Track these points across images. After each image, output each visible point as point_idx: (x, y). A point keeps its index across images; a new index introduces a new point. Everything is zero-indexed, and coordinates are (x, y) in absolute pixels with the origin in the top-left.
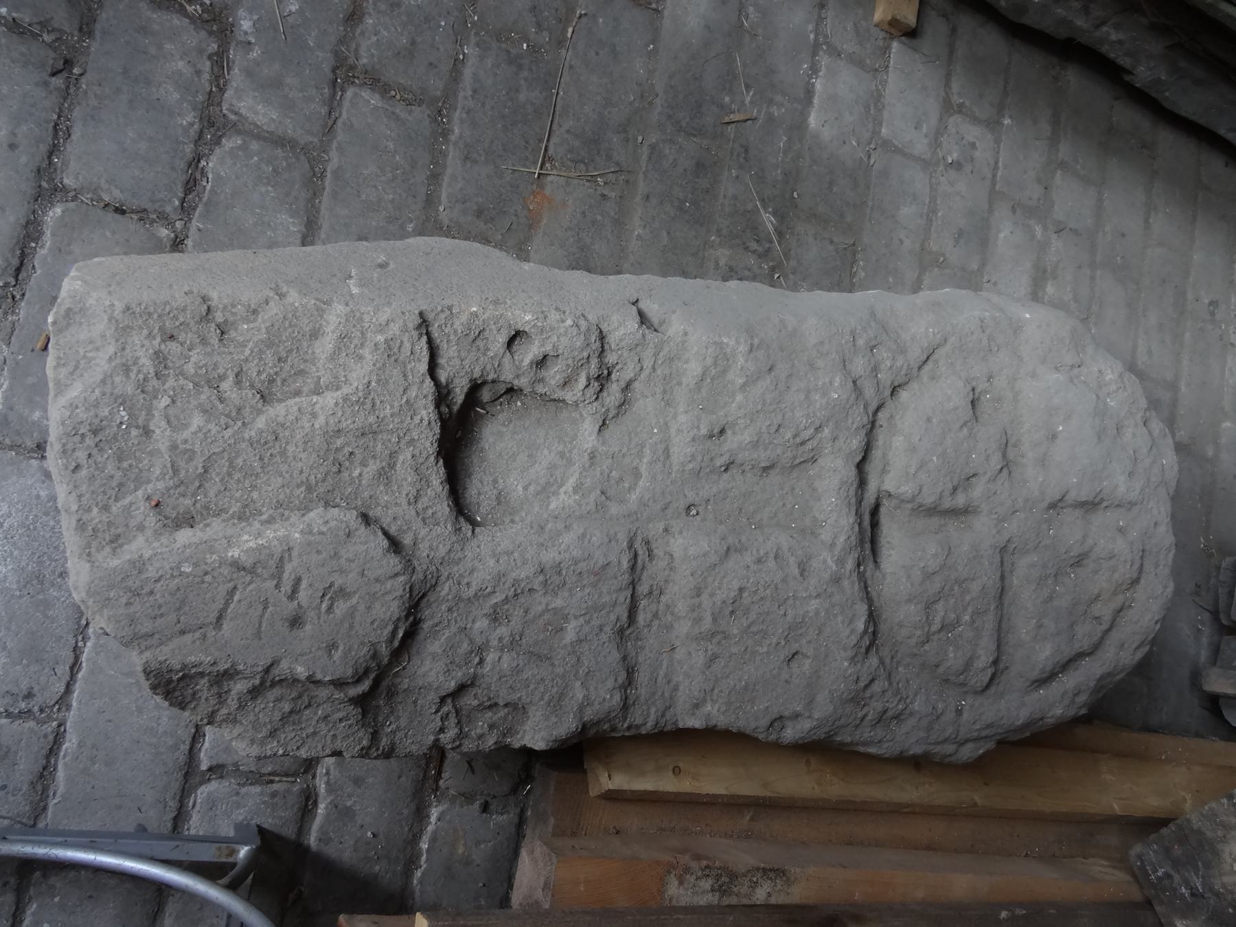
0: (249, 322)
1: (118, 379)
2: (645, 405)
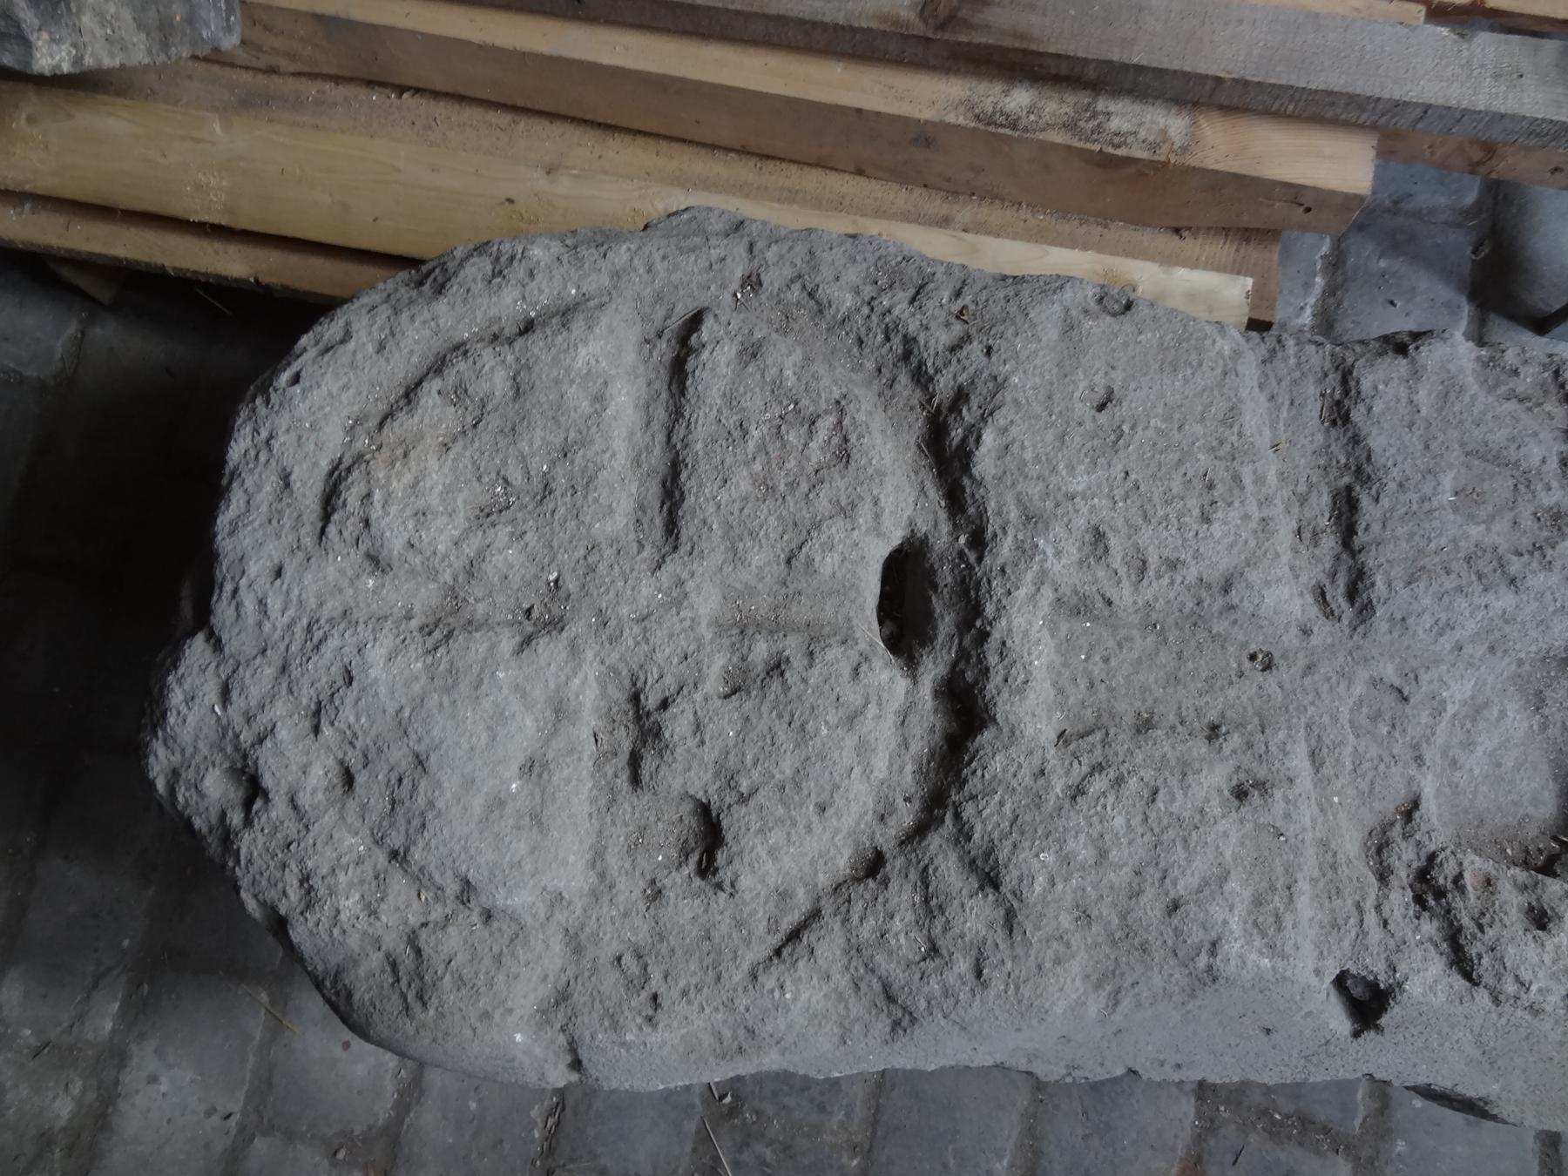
2: (1351, 844)
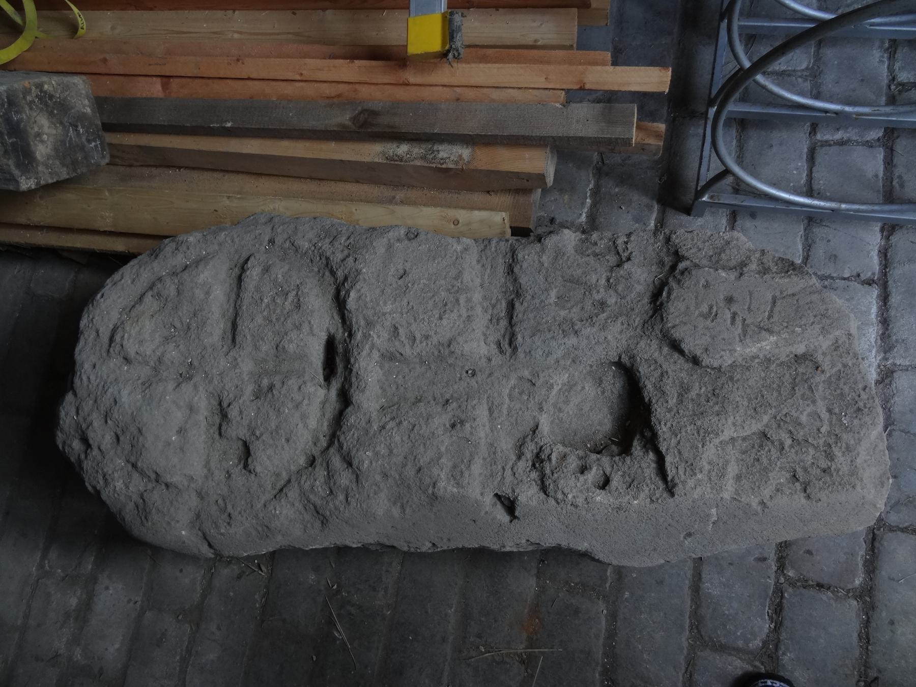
0: (780, 484)
1: (852, 442)
2: (506, 445)
